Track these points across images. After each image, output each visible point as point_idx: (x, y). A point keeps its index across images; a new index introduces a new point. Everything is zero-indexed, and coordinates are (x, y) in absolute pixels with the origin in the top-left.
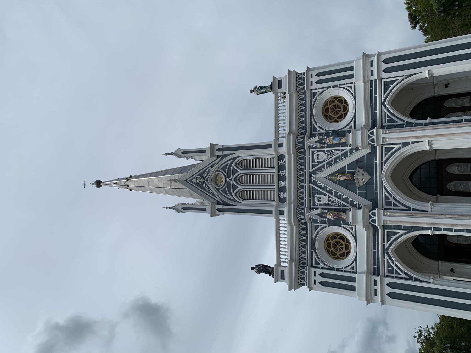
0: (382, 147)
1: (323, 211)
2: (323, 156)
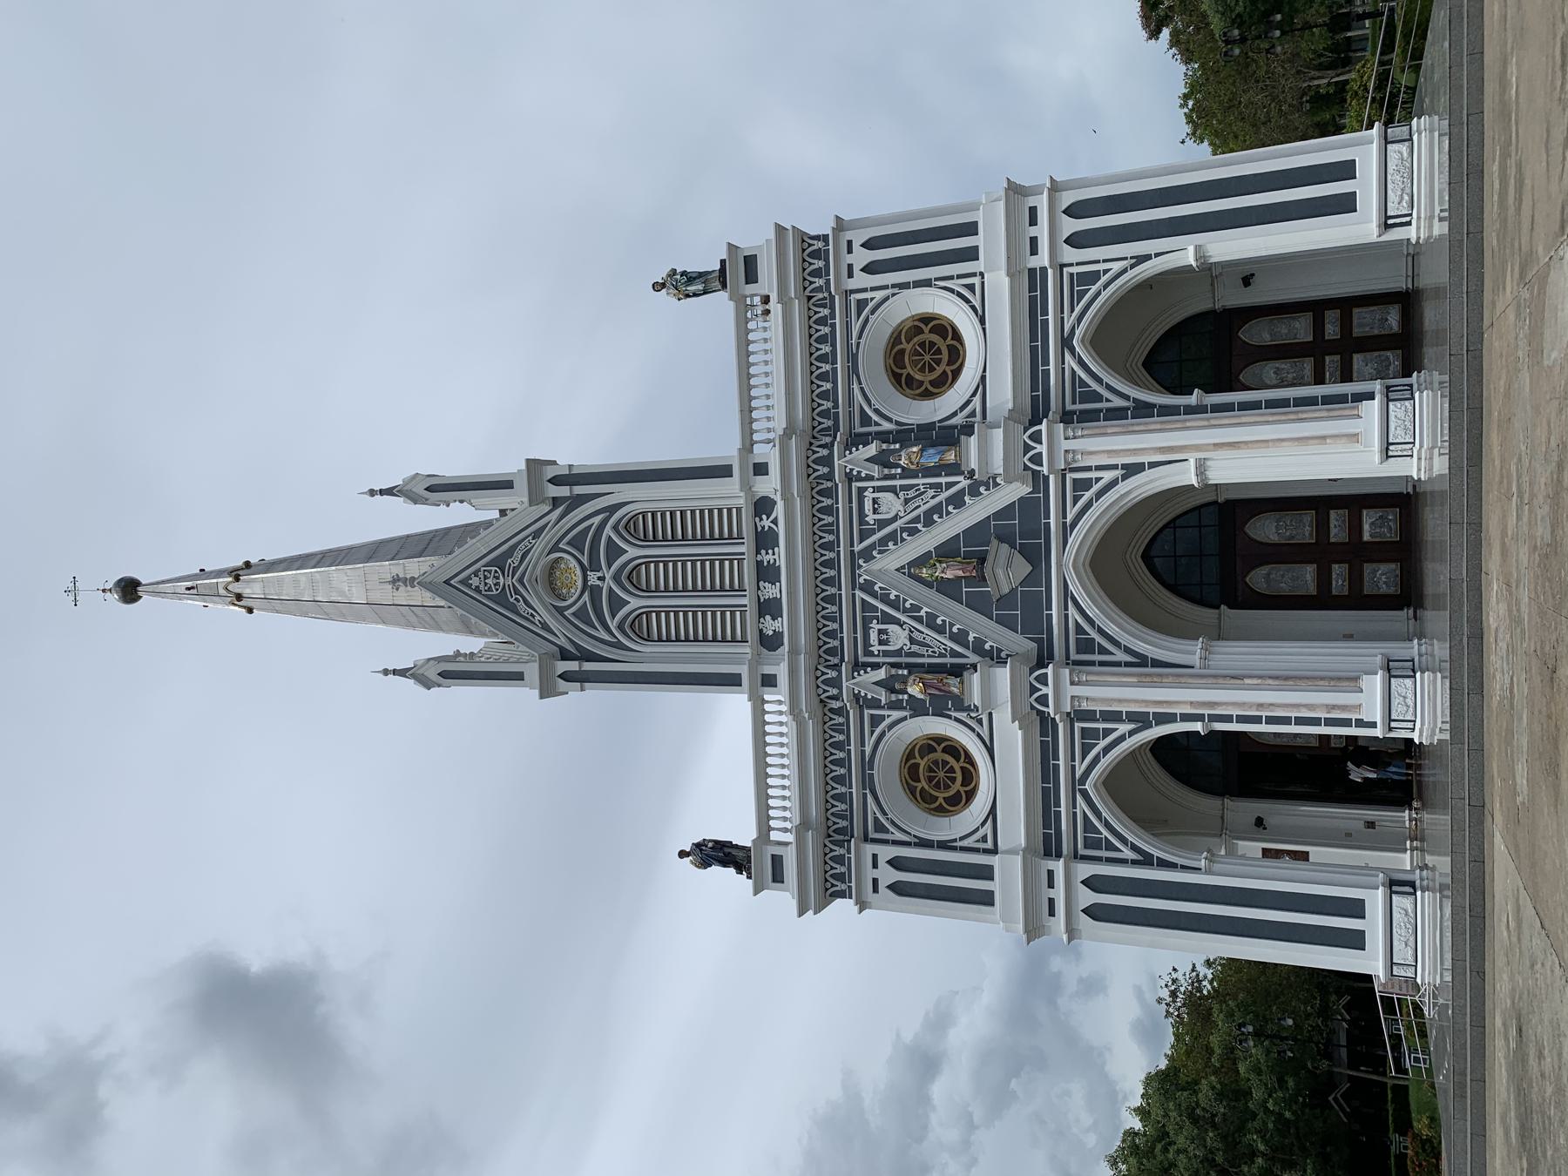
0: (1064, 477)
1: (893, 671)
2: (891, 504)
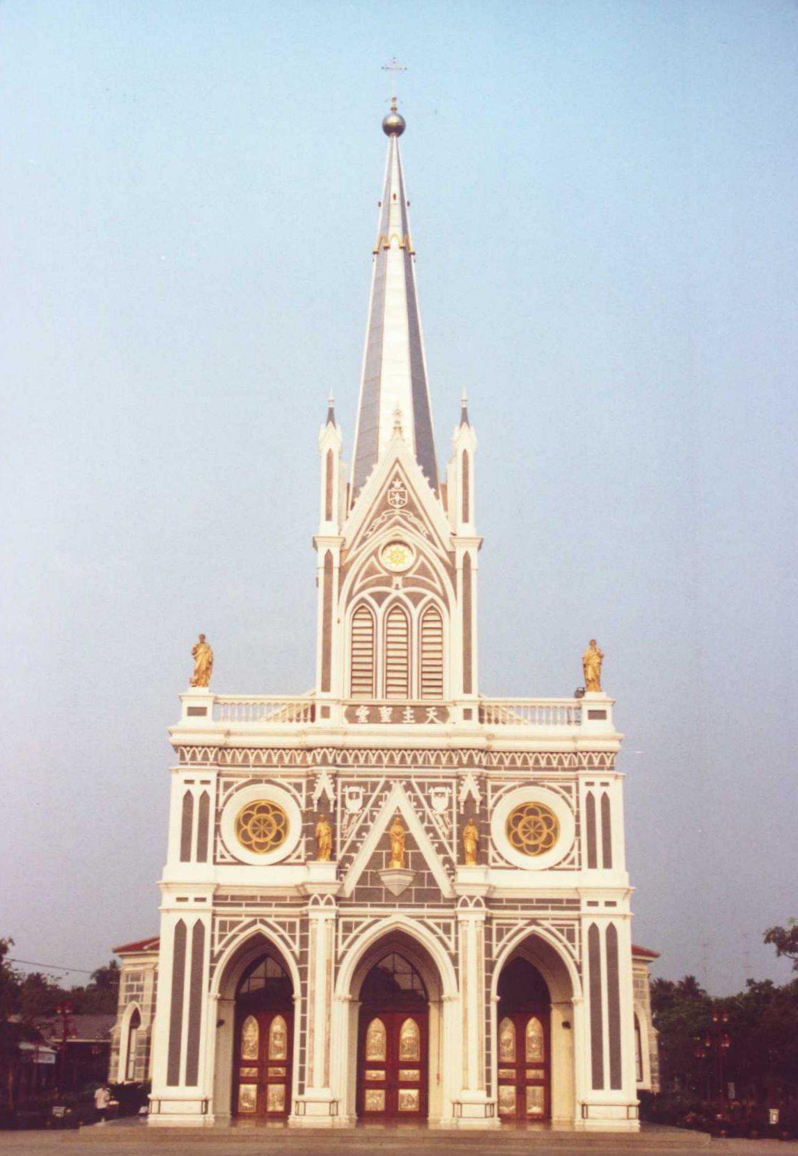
1: (332, 803)
2: (440, 804)
